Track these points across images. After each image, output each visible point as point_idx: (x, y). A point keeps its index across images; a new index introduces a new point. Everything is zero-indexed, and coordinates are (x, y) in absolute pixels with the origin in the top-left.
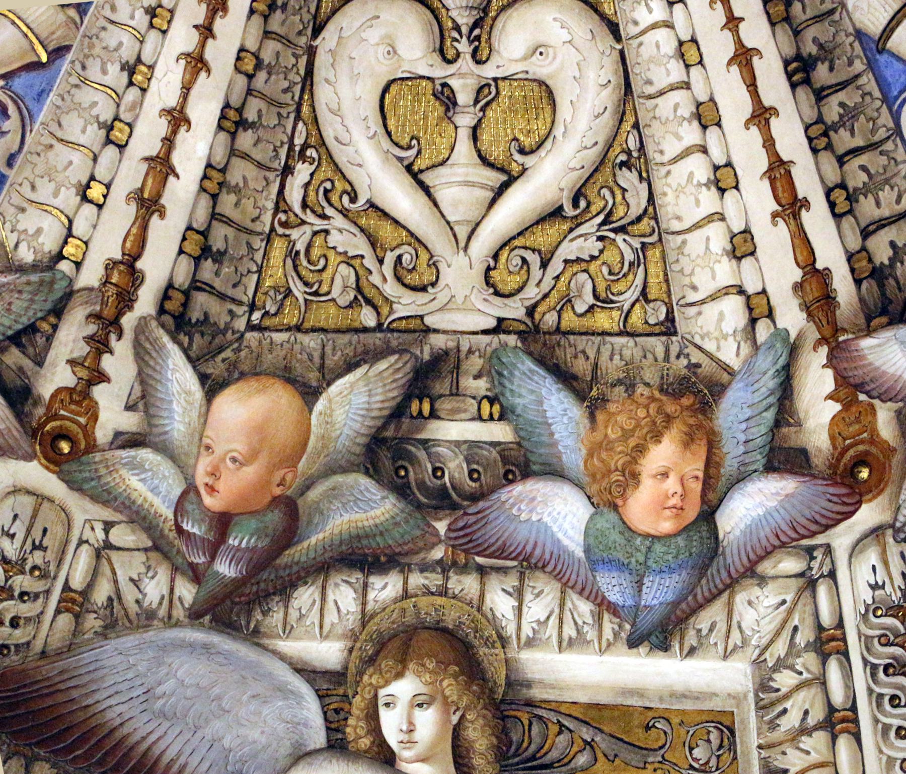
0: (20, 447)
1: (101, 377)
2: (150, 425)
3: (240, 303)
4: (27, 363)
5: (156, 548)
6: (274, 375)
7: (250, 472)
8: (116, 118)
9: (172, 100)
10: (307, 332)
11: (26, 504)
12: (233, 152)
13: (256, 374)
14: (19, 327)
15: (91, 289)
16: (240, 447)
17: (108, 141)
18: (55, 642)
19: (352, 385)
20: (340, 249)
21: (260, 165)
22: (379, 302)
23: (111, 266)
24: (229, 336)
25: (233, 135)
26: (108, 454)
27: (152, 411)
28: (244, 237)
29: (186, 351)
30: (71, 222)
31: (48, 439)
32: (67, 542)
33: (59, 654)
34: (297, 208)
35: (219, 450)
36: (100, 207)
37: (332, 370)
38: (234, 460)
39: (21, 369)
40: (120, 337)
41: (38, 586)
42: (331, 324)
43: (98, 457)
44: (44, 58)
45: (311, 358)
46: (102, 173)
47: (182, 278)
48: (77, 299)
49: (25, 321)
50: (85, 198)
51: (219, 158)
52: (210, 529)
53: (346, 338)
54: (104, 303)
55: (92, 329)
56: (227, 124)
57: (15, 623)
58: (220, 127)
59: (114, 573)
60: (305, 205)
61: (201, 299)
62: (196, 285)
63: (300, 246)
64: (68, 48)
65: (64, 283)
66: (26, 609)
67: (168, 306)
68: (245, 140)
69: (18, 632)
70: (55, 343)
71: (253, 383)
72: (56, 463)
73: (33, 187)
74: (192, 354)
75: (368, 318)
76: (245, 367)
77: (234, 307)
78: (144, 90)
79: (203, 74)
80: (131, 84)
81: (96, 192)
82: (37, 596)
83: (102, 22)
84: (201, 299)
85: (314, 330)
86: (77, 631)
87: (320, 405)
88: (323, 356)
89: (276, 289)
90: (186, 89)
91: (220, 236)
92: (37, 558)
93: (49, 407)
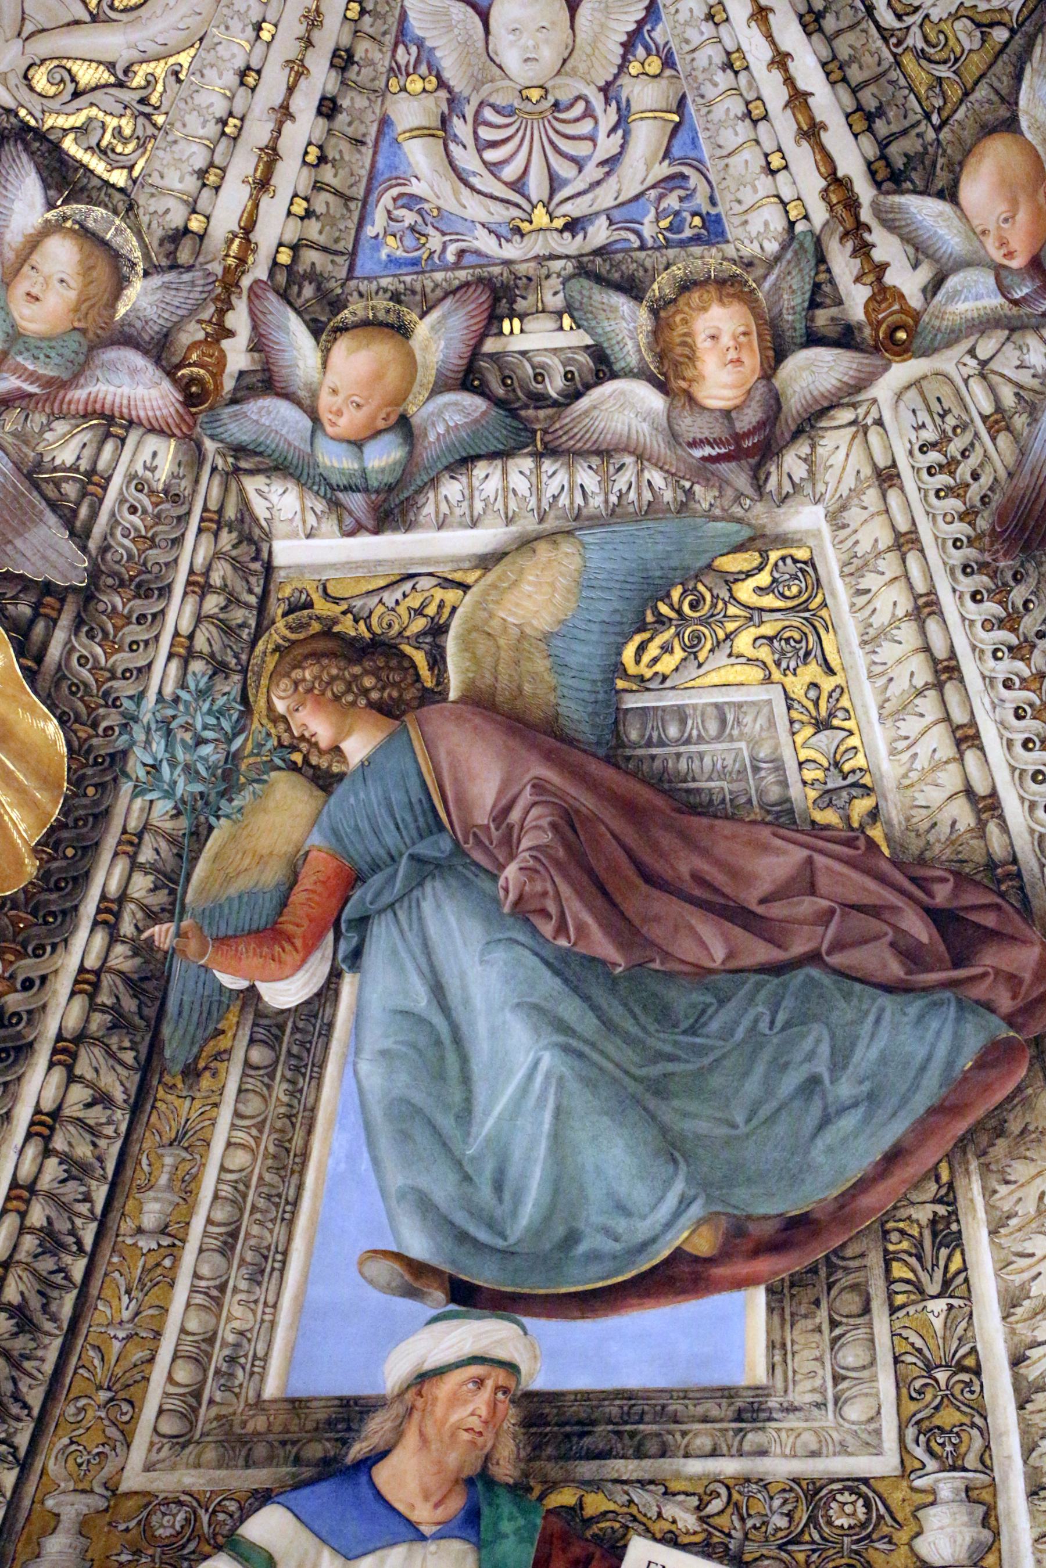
0: (876, 366)
1: (881, 268)
2: (937, 261)
3: (919, 122)
4: (833, 311)
5: (1013, 330)
6: (978, 141)
7: (1023, 216)
8: (747, 103)
9: (767, 54)
10: (973, 90)
11: (913, 393)
12: (829, 40)
13: (968, 152)
14: (807, 296)
15: (827, 223)
16: (1002, 208)
17: (755, 122)
18: (1010, 460)
19: (1031, 87)
20: (945, 16)
21: (852, 27)
22: (998, 17)
23: (825, 194)
24: (931, 150)
25: (820, 30)
26: (931, 309)
27: (930, 252)
28: (883, 80)
29: (915, 192)
30: (778, 196)
31: (887, 342)
32: (958, 391)
33: (1019, 463)
34: (897, 25)
35: (991, 227)
36: (786, 167)
37: (1010, 94)
38: (1006, 220)
39: (833, 319)
40: (870, 231)
41: (967, 438)
42: (983, 67)
43: (926, 318)
44: (677, 119)
45: (990, 102)
46: (768, 146)
47: (871, 150)
48: (824, 239)
49: (808, 287)
50: (773, 173)
51: (825, 53)
52: (1033, 279)
53: (1000, 63)
54: (842, 222)
55: (849, 245)
56: (811, 27)
57: (975, 476)
58: (809, 34)
59: (1003, 376)
60: (899, 17)
61: (895, 150)
62: (883, 145)
63: (920, 44)
64: (684, 97)
65: (809, 238)
66: (974, 460)
67: (880, 177)
68: (830, 23)
69: (983, 480)
70: (837, 280)
71: (972, 160)
72: (906, 351)
73: (739, 202)
74: (921, 188)
75: (1000, 35)
76: (959, 157)
77: (917, 130)
78: (747, 68)
79: (771, 16)
80: (736, 73)
81: (776, 162)
82: (972, 445)
83: (688, 57)
84: (895, 150)
85: (976, 83)
86: (1016, 440)
87: (1024, 123)
88: (997, 92)
89: (931, 88)
90: (769, 37)
91: (869, 100)
92: (951, 421)
93: (871, 324)
